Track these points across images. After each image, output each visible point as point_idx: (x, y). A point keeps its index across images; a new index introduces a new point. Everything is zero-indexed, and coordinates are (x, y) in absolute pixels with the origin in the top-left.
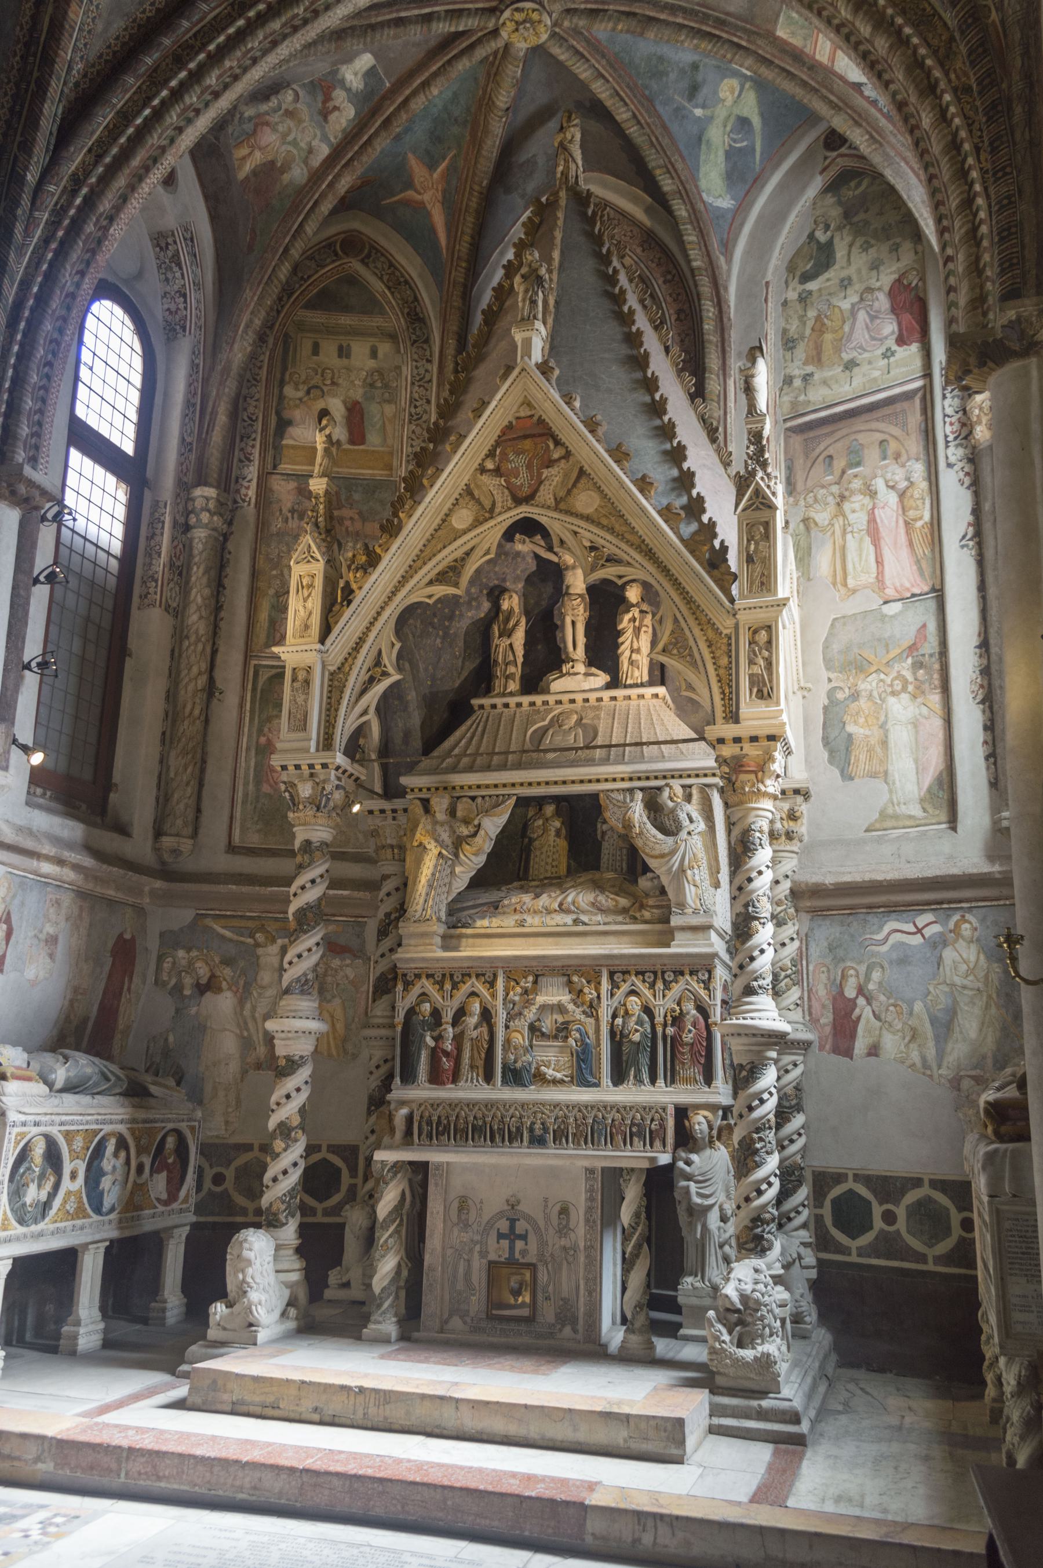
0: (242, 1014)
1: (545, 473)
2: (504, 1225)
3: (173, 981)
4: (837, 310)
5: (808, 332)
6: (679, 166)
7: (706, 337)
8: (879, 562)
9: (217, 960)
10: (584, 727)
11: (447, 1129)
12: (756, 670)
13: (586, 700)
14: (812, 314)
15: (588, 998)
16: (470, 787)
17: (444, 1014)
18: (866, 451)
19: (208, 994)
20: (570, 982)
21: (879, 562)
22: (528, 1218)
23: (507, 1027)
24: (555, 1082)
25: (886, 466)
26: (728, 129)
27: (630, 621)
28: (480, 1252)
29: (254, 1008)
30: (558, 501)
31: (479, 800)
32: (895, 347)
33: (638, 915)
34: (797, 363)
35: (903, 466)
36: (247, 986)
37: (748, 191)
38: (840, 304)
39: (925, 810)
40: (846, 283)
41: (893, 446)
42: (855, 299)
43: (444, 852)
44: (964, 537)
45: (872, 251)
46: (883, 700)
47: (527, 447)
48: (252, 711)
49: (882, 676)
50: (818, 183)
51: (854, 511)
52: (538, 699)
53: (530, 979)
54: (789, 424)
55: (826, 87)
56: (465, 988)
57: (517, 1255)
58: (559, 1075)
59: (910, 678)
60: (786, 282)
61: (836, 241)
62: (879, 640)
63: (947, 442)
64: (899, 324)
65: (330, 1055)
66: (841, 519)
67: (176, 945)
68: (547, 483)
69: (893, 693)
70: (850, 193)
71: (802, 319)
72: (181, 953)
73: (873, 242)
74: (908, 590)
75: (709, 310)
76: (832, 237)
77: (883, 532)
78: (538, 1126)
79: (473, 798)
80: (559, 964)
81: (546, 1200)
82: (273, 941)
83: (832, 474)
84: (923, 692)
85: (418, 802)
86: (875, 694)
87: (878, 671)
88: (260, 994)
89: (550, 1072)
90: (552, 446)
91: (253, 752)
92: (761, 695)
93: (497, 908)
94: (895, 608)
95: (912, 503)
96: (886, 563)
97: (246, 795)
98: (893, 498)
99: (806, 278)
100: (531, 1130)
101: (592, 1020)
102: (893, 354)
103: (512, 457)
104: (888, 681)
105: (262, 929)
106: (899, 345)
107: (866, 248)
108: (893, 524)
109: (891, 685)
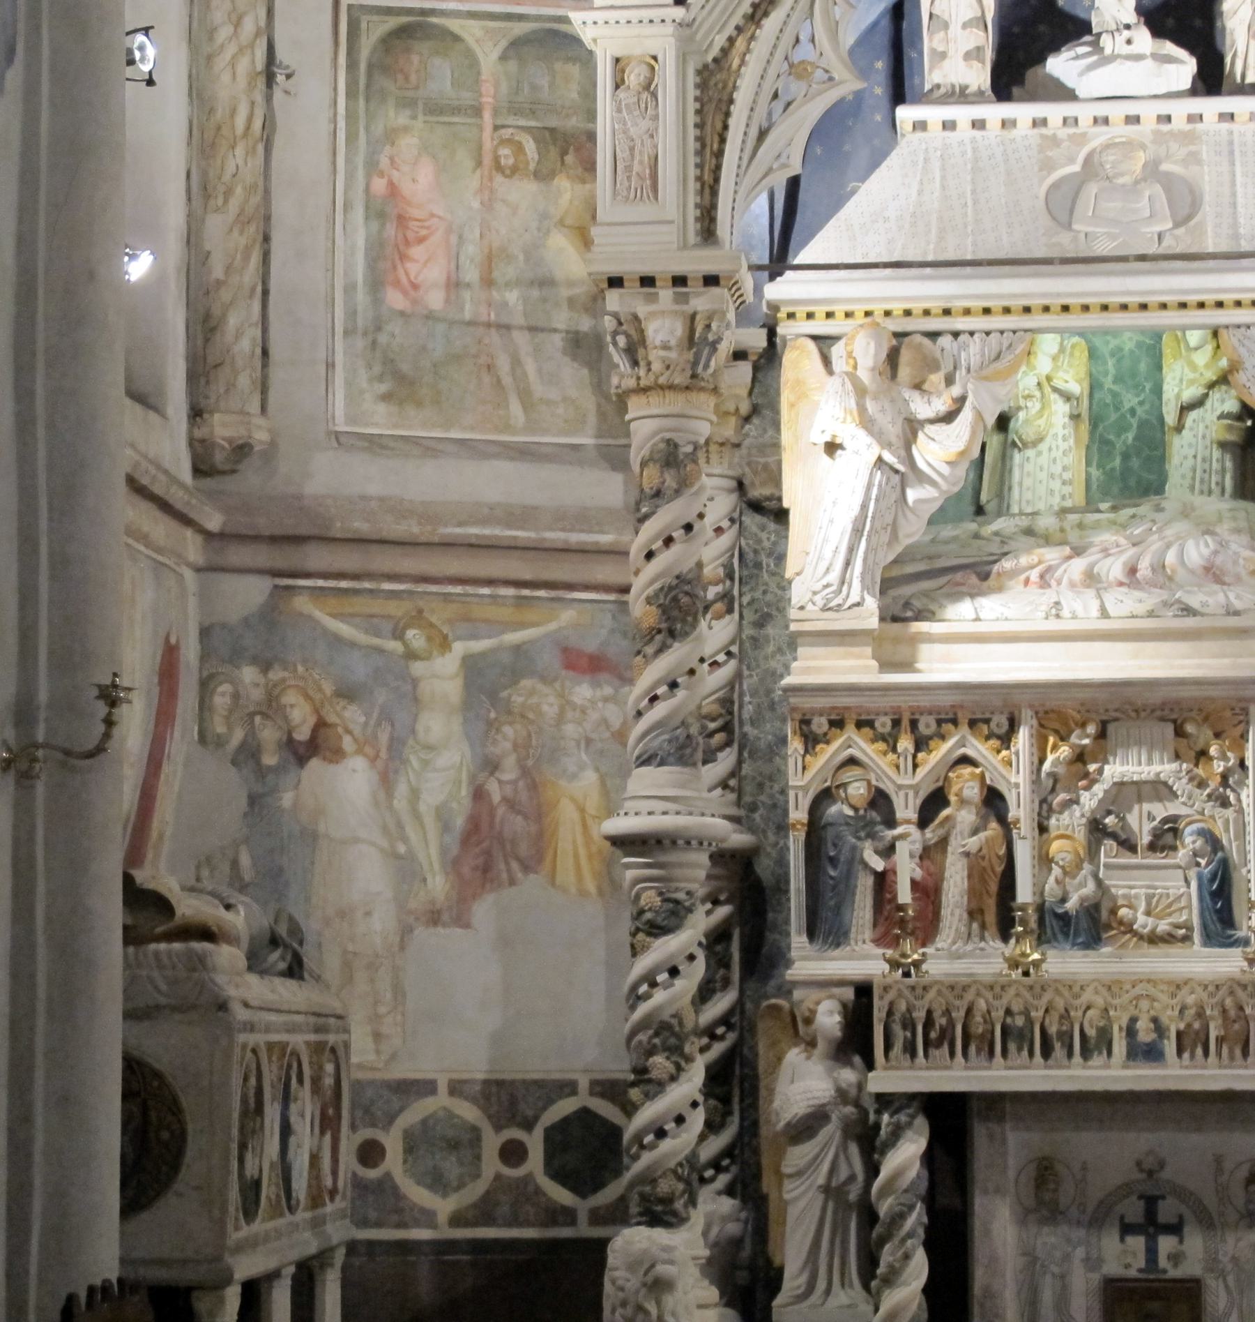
0: (390, 807)
2: (1134, 1210)
3: (238, 736)
9: (328, 688)
10: (1168, 182)
11: (946, 1035)
15: (1219, 767)
16: (927, 313)
17: (898, 802)
19: (314, 763)
20: (1179, 732)
22: (1182, 1194)
23: (1043, 829)
24: (1154, 939)
28: (1087, 1260)
29: (415, 794)
31: (945, 341)
36: (396, 746)
43: (888, 457)
48: (351, 116)
52: (1054, 112)
53: (1091, 729)
56: (941, 751)
57: (1163, 1262)
58: (1163, 926)
65: (583, 893)
67: (236, 656)
72: (249, 674)
78: (1143, 1025)
79: (933, 335)
80: (1156, 697)
81: (1218, 1160)
82: (445, 644)
85: (811, 346)
88: (425, 763)
89: (1142, 922)
91: (359, 213)
93: (985, 577)
97: (351, 314)
100: (1131, 1032)
101: (1230, 813)
105: (418, 619)
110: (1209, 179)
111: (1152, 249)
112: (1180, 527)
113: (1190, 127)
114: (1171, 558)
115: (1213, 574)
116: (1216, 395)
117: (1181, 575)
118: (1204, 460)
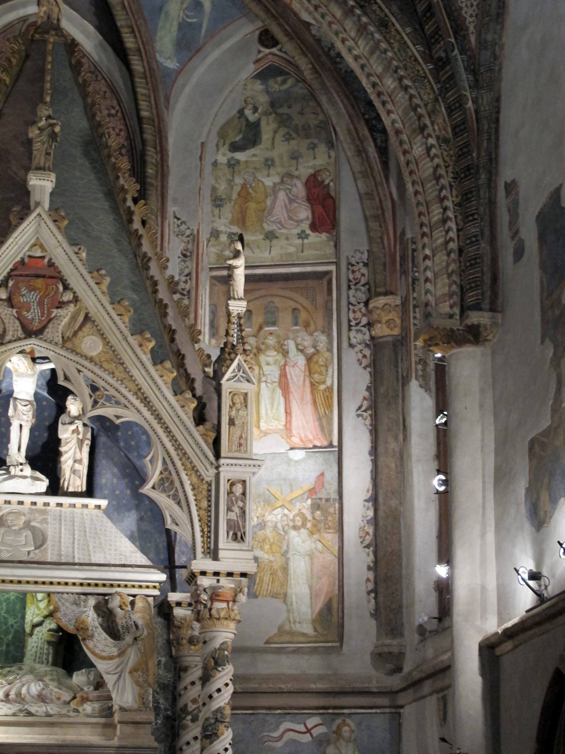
1: (55, 312)
4: (260, 184)
5: (234, 196)
6: (143, 29)
7: (149, 180)
8: (288, 412)
10: (34, 530)
12: (232, 516)
13: (34, 504)
14: (238, 181)
18: (281, 314)
21: (288, 412)
25: (298, 331)
26: (185, 6)
27: (73, 432)
30: (65, 340)
32: (308, 231)
33: (80, 709)
34: (223, 221)
35: (311, 334)
37: (191, 58)
38: (264, 180)
39: (315, 630)
40: (269, 163)
41: (303, 315)
42: (277, 179)
44: (360, 408)
45: (293, 142)
46: (286, 532)
47: (39, 286)
49: (286, 511)
50: (251, 69)
51: (268, 364)
54: (215, 273)
55: (283, 18)
59: (309, 517)
60: (217, 146)
61: (263, 123)
62: (285, 480)
63: (350, 326)
64: (313, 213)
66: (256, 368)
68: (54, 321)
69: (295, 528)
70: (275, 85)
71: (230, 182)
73: (294, 135)
74: (311, 441)
75: (152, 156)
76: (259, 120)
77: (292, 388)
83: (250, 327)
84: (319, 531)
86: (279, 526)
87: (282, 506)
90: (61, 288)
92: (235, 538)
94: (299, 455)
95: (316, 367)
96: (293, 415)
98: (301, 361)
99: (235, 147)
102: (307, 236)
103: (24, 291)
104: (291, 517)
106: (312, 230)
107: (288, 138)
108: (301, 383)
109: (293, 520)
110: (51, 530)
111: (25, 558)
112: (29, 677)
113: (44, 508)
114: (24, 691)
115: (41, 698)
116: (47, 621)
117: (28, 698)
118: (41, 648)
